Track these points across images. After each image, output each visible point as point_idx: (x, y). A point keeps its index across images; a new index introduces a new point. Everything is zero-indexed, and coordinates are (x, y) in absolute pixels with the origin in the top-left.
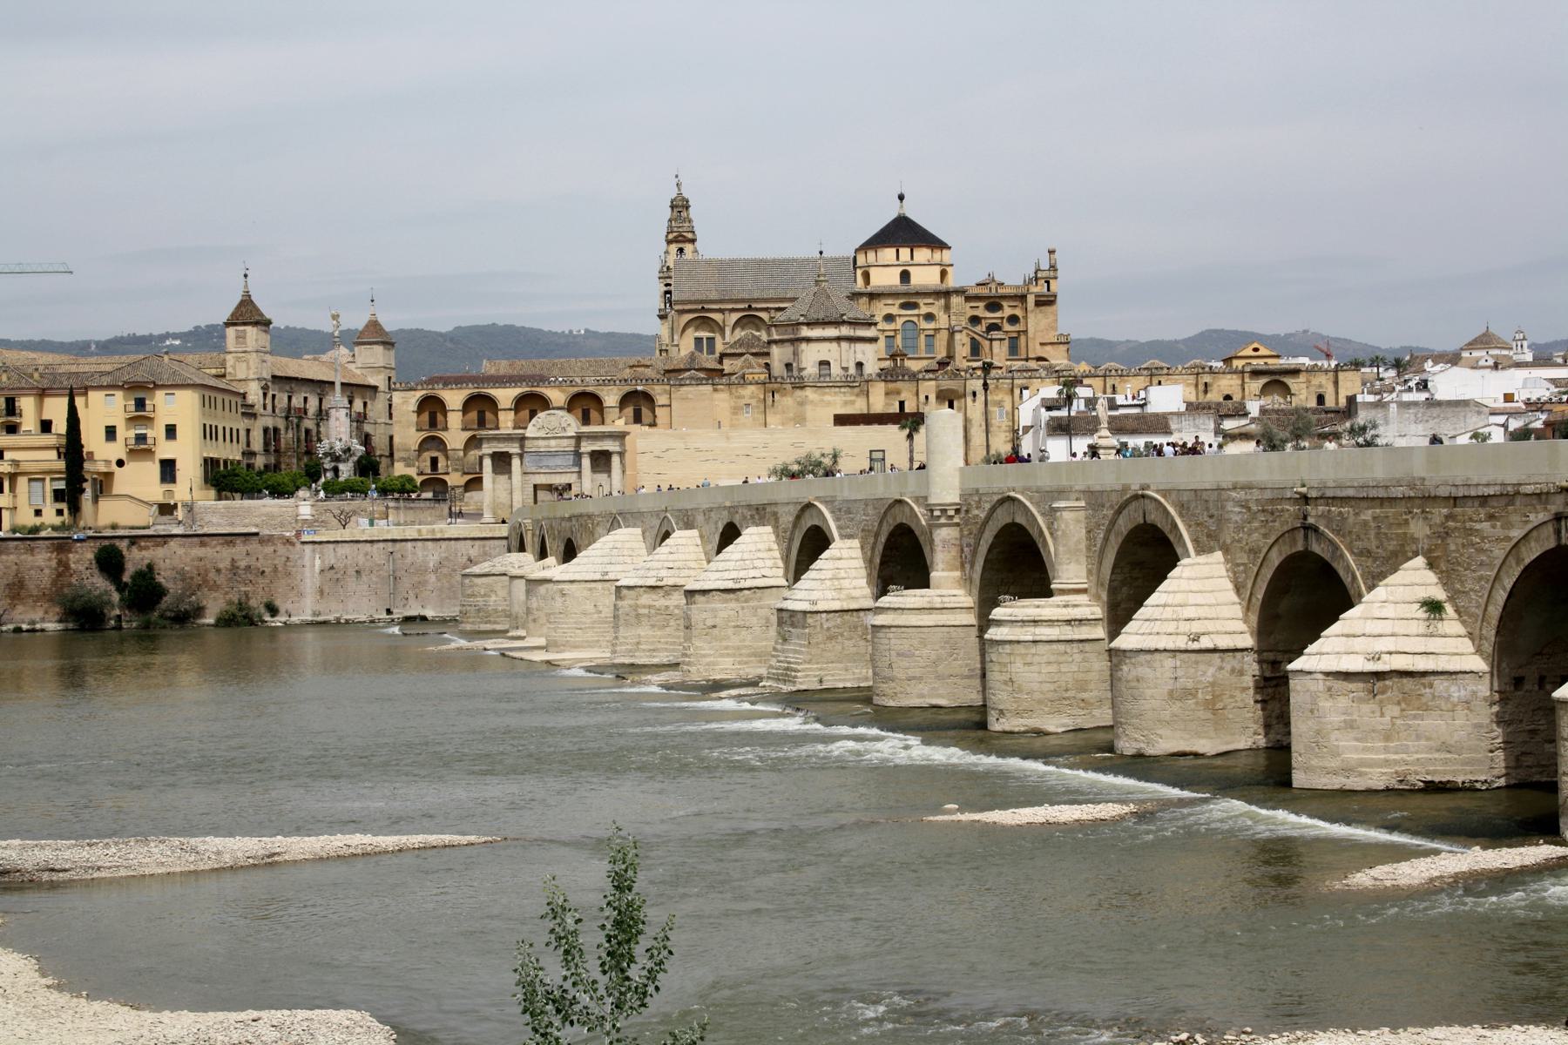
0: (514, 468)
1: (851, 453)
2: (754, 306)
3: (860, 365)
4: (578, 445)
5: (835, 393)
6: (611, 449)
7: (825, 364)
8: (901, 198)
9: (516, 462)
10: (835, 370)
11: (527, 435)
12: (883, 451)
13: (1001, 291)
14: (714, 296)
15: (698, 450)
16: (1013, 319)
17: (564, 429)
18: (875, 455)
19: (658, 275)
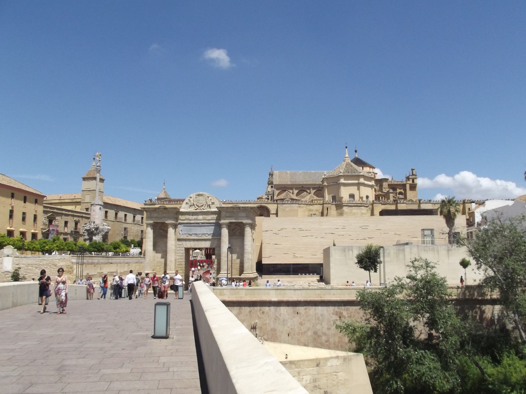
0: (169, 235)
1: (398, 233)
2: (304, 187)
3: (367, 197)
4: (219, 219)
5: (358, 209)
6: (244, 221)
7: (352, 196)
8: (356, 151)
9: (171, 231)
10: (357, 198)
11: (182, 210)
12: (432, 230)
13: (395, 183)
14: (289, 183)
15: (301, 230)
16: (400, 193)
17: (209, 206)
18: (426, 233)
19: (265, 193)
